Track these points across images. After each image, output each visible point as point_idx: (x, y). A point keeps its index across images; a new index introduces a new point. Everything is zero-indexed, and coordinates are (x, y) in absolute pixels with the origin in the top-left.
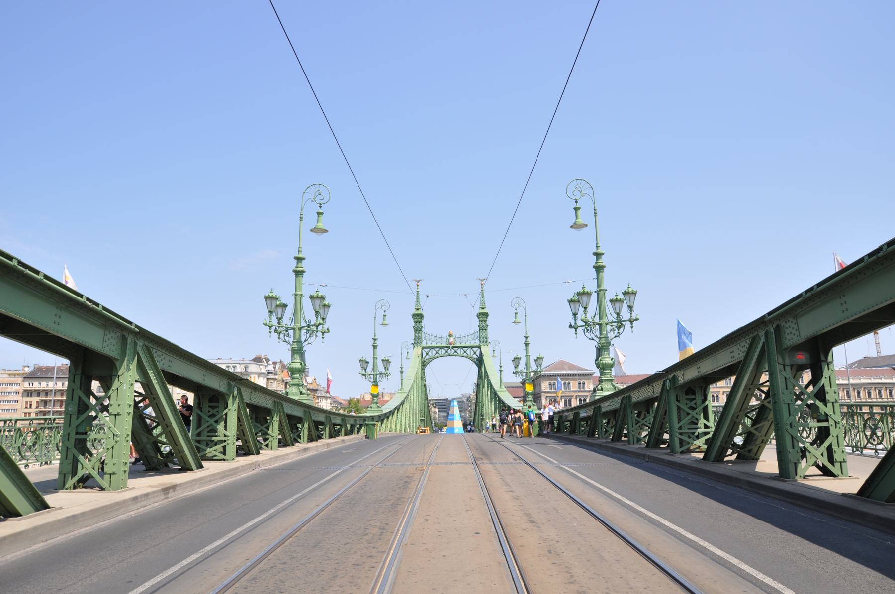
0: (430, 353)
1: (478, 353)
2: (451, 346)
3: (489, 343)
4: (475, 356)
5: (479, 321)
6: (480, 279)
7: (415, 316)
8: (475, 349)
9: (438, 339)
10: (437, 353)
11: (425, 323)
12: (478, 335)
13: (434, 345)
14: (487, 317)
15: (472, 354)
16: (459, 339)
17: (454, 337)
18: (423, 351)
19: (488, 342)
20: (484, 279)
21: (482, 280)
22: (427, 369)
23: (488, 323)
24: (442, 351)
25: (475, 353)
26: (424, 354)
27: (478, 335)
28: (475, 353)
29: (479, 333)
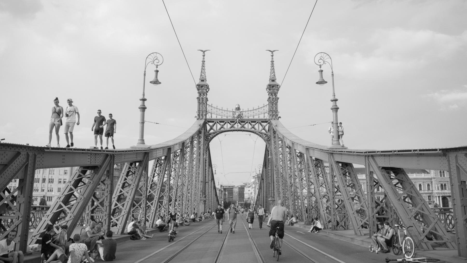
0: (215, 127)
1: (267, 128)
3: (280, 117)
4: (263, 131)
6: (270, 51)
7: (199, 87)
8: (264, 124)
11: (210, 95)
13: (219, 117)
16: (247, 113)
18: (207, 124)
22: (212, 144)
23: (278, 95)
24: (228, 126)
26: (208, 128)
27: (267, 109)
28: (264, 129)
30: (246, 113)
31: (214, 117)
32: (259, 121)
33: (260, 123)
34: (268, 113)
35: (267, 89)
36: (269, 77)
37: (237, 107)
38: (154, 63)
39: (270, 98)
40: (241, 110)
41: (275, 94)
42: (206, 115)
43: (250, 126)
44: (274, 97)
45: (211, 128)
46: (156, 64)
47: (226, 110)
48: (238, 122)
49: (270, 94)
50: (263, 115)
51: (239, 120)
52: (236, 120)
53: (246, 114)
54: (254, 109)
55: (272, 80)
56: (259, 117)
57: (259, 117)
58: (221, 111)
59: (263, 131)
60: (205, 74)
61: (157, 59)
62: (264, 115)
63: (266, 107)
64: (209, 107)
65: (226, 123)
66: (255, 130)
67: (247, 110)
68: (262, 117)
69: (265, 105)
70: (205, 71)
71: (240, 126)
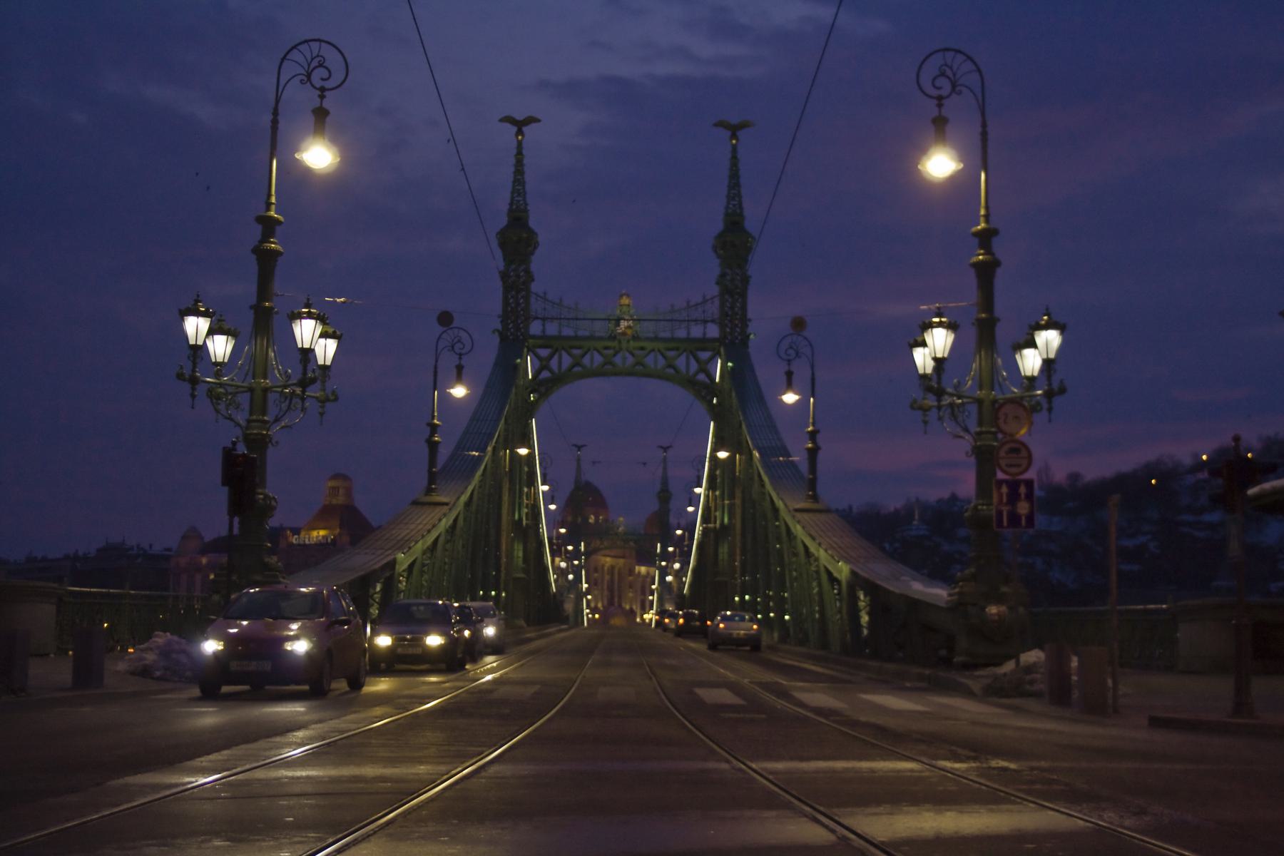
0: (554, 363)
11: (537, 263)
27: (714, 309)
29: (717, 302)
31: (552, 329)
39: (723, 275)
46: (318, 84)
56: (689, 333)
57: (689, 333)
61: (321, 65)
63: (713, 303)
68: (696, 332)
69: (708, 297)
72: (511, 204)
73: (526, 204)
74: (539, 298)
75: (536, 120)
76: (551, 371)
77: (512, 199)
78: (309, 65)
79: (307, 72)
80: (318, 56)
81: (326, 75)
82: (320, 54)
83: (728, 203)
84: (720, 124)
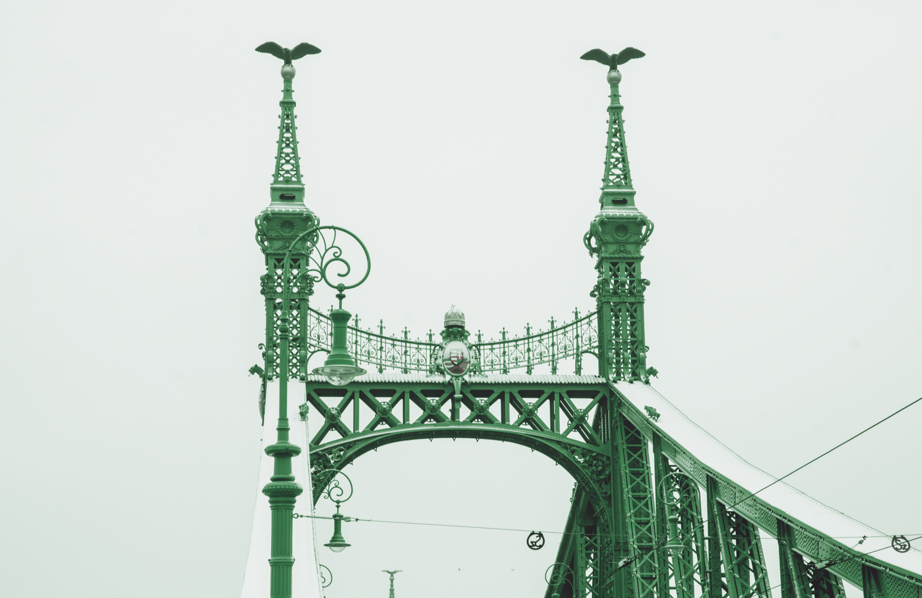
0: (346, 419)
2: (458, 384)
3: (653, 372)
4: (575, 436)
5: (599, 266)
8: (581, 404)
9: (388, 346)
10: (384, 416)
12: (595, 336)
14: (642, 242)
15: (562, 431)
17: (472, 340)
19: (648, 367)
20: (631, 54)
21: (613, 62)
23: (646, 270)
25: (578, 422)
27: (590, 331)
29: (595, 323)
30: (492, 349)
32: (557, 390)
33: (561, 398)
34: (596, 351)
35: (589, 239)
36: (602, 184)
37: (451, 323)
38: (323, 276)
40: (472, 340)
41: (630, 264)
42: (304, 361)
43: (514, 415)
44: (623, 277)
45: (333, 422)
47: (401, 336)
48: (458, 395)
49: (606, 266)
50: (571, 362)
51: (465, 384)
52: (450, 384)
53: (492, 357)
54: (533, 332)
55: (612, 198)
56: (554, 370)
57: (554, 370)
58: (375, 343)
59: (575, 436)
60: (297, 167)
61: (337, 258)
62: (578, 361)
63: (589, 324)
64: (320, 321)
65: (402, 396)
66: (538, 433)
67: (499, 338)
70: (295, 151)
71: (465, 412)
72: (277, 175)
73: (298, 175)
74: (321, 318)
75: (314, 50)
76: (343, 432)
77: (278, 167)
78: (322, 258)
79: (321, 268)
80: (333, 247)
81: (343, 269)
82: (334, 245)
83: (608, 170)
84: (596, 55)
